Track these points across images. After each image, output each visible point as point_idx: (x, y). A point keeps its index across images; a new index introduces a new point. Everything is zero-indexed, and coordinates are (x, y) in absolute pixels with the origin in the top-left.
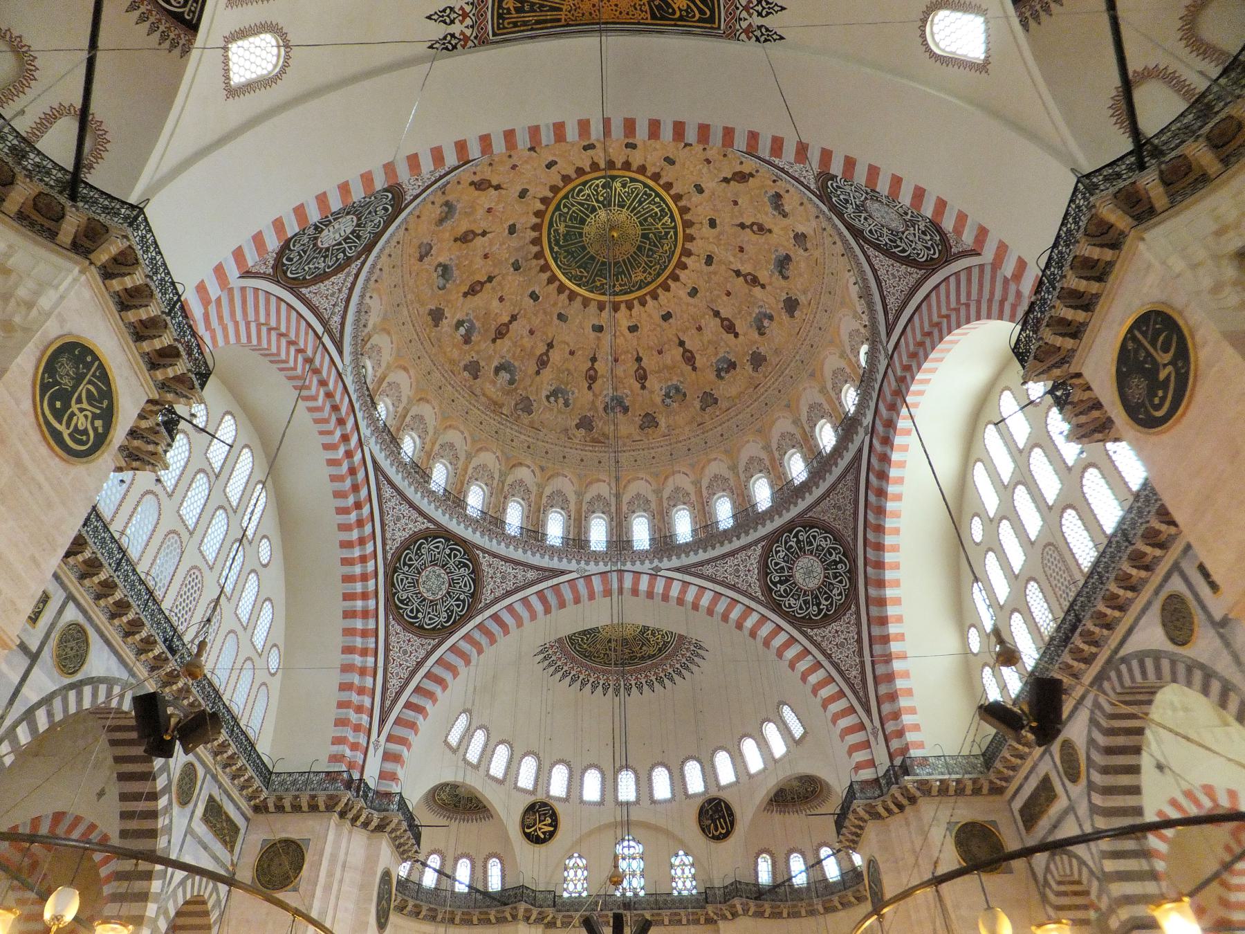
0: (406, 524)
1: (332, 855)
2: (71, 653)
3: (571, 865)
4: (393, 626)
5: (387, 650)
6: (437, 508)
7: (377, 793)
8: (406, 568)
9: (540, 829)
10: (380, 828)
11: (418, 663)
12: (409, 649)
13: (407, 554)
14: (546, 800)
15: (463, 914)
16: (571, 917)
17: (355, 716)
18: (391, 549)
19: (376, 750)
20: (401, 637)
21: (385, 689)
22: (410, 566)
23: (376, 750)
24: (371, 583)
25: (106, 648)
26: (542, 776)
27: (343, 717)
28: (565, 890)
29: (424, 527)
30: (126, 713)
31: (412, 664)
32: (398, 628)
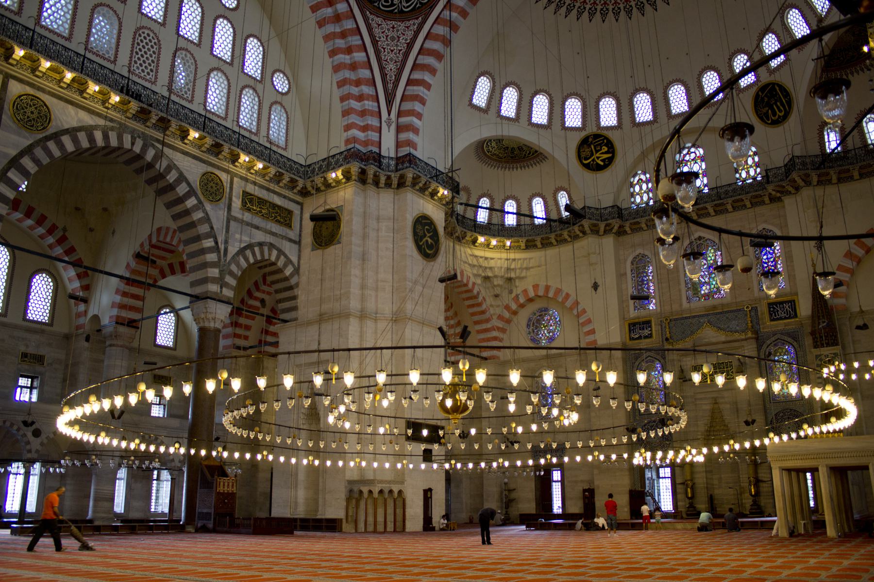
3: (635, 182)
4: (373, 20)
5: (375, 42)
7: (398, 159)
9: (598, 158)
10: (401, 184)
11: (408, 44)
12: (395, 34)
14: (599, 132)
15: (542, 239)
16: (638, 223)
17: (359, 104)
19: (389, 128)
20: (383, 27)
21: (384, 76)
23: (389, 128)
26: (590, 112)
27: (347, 107)
28: (633, 203)
31: (403, 47)
32: (379, 20)
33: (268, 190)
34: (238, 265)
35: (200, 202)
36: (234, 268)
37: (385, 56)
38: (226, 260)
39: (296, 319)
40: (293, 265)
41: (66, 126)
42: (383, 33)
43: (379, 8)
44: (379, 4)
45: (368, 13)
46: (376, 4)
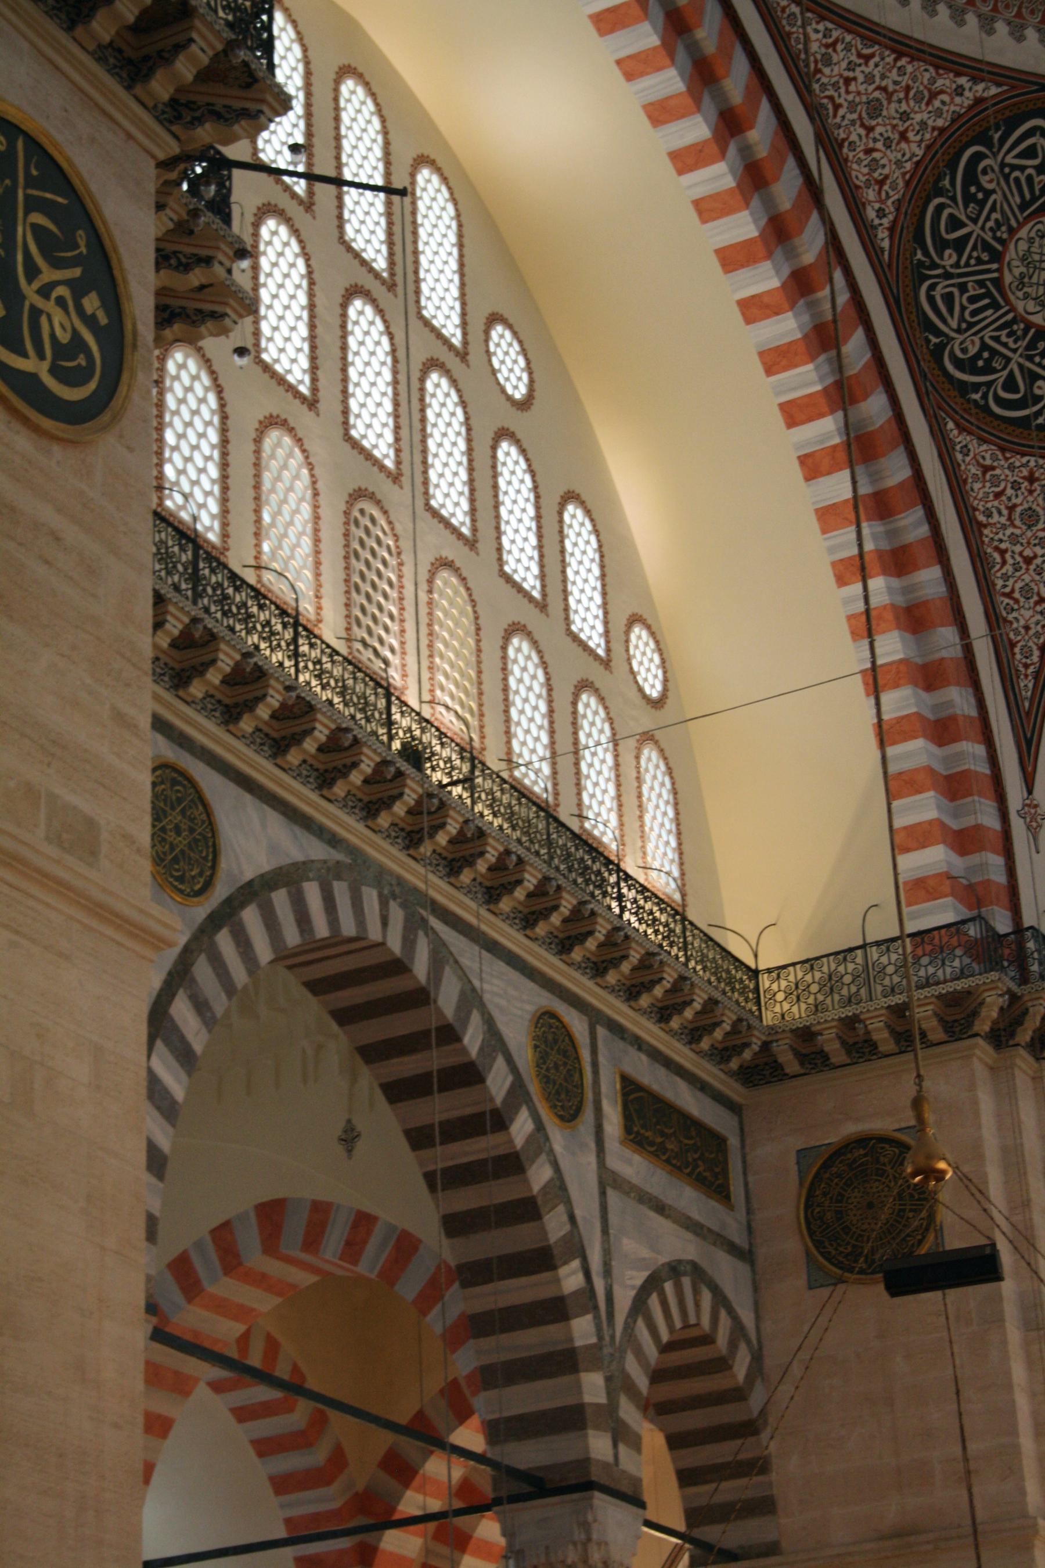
0: (905, 116)
1: (1005, 1150)
2: (182, 841)
5: (971, 528)
6: (987, 26)
8: (949, 258)
13: (940, 208)
18: (881, 213)
21: (1003, 650)
22: (959, 245)
24: (855, 347)
25: (248, 797)
29: (966, 100)
30: (351, 940)
32: (986, 452)
33: (668, 1064)
34: (639, 1353)
35: (540, 1126)
36: (632, 1366)
37: (1006, 577)
38: (613, 1337)
39: (772, 1549)
40: (748, 1342)
41: (249, 874)
42: (998, 495)
43: (986, 409)
44: (985, 396)
45: (951, 425)
46: (976, 396)
